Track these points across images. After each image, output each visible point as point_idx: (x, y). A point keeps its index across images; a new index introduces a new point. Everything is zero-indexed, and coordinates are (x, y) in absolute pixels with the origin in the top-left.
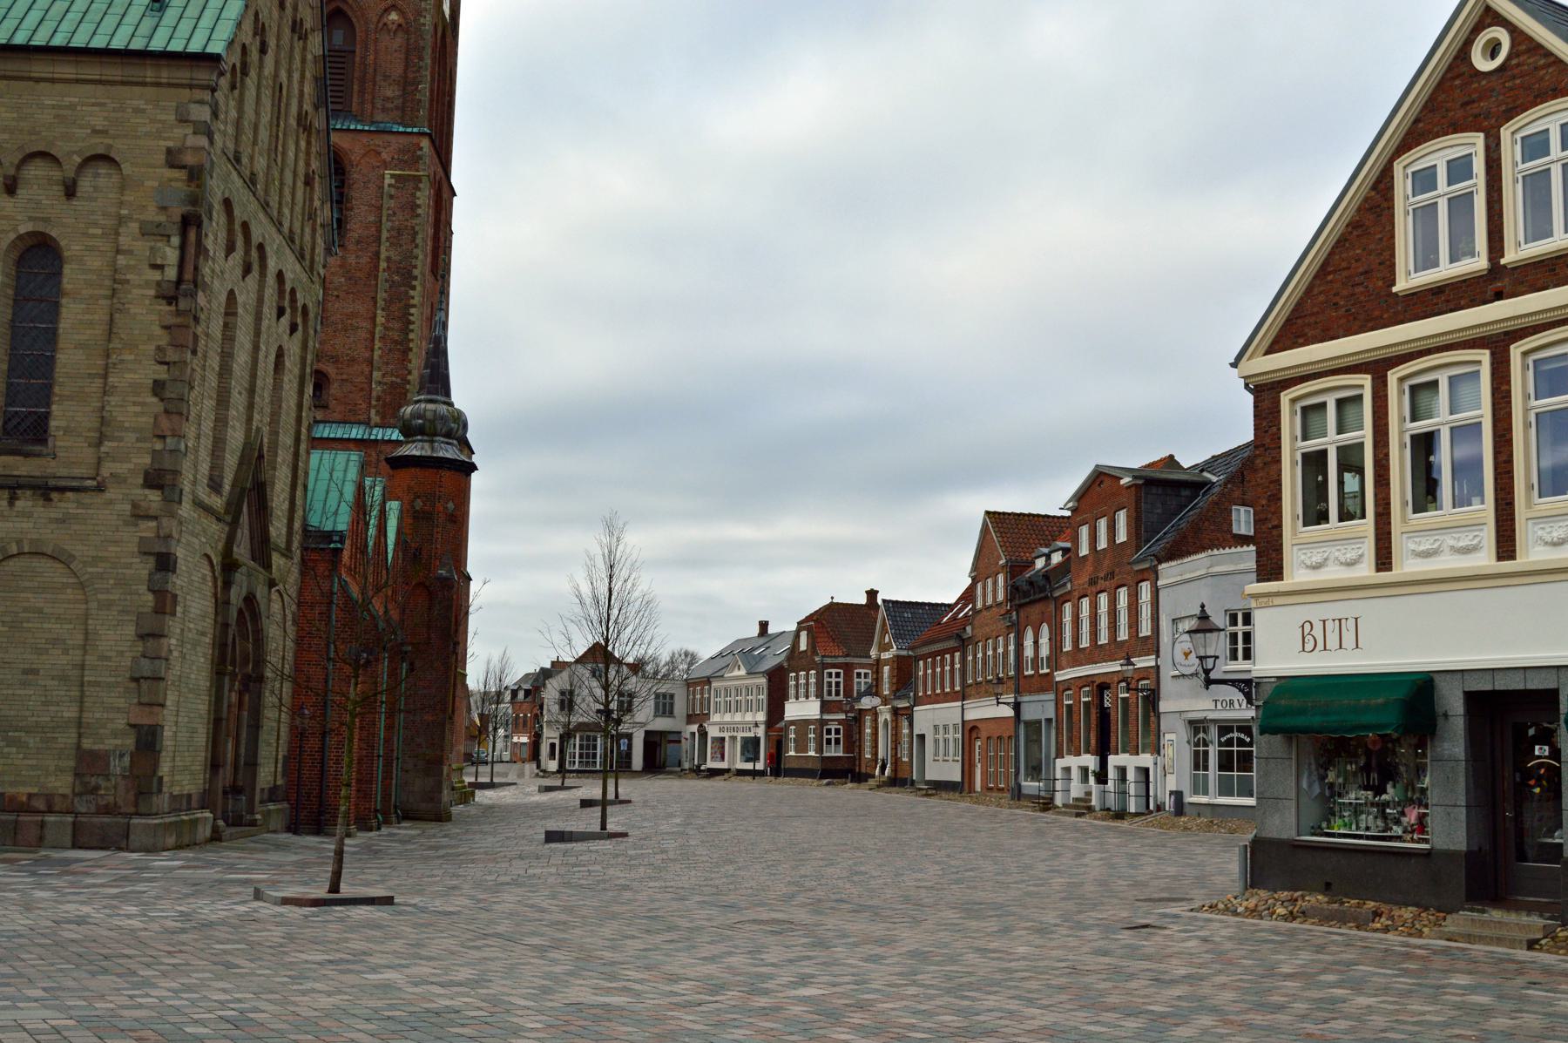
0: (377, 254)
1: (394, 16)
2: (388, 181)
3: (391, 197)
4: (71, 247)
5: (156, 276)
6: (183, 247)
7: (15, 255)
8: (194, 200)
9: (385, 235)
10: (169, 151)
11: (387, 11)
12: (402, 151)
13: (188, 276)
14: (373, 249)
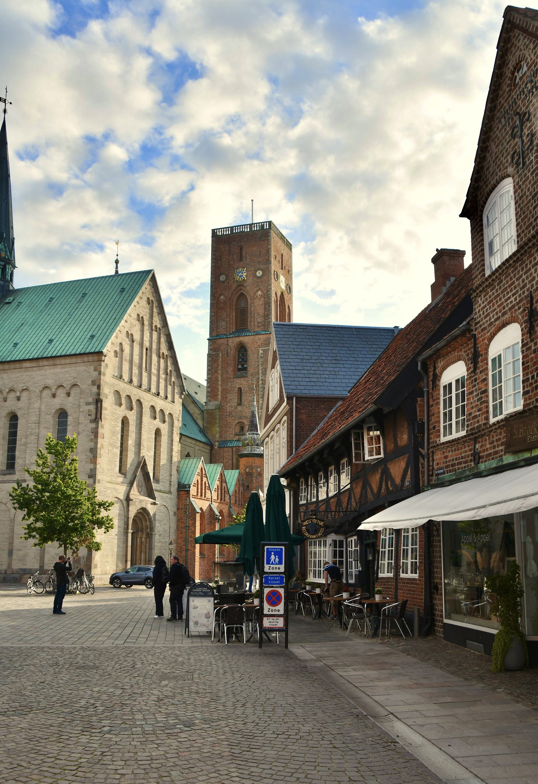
0: (258, 378)
1: (259, 293)
2: (261, 352)
3: (262, 357)
4: (70, 412)
5: (90, 418)
6: (97, 408)
7: (57, 416)
8: (99, 394)
9: (260, 372)
10: (92, 381)
11: (257, 291)
12: (265, 341)
13: (99, 416)
14: (257, 377)
